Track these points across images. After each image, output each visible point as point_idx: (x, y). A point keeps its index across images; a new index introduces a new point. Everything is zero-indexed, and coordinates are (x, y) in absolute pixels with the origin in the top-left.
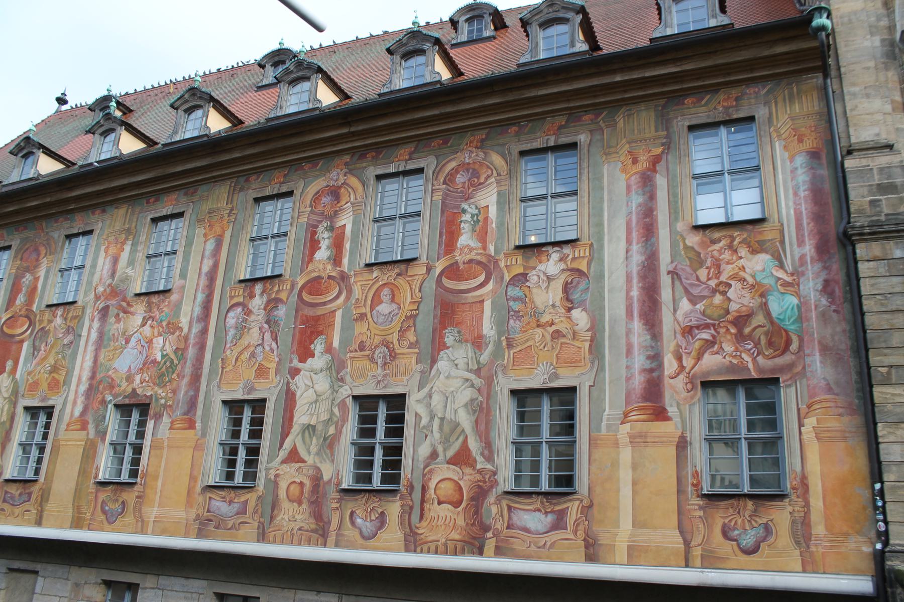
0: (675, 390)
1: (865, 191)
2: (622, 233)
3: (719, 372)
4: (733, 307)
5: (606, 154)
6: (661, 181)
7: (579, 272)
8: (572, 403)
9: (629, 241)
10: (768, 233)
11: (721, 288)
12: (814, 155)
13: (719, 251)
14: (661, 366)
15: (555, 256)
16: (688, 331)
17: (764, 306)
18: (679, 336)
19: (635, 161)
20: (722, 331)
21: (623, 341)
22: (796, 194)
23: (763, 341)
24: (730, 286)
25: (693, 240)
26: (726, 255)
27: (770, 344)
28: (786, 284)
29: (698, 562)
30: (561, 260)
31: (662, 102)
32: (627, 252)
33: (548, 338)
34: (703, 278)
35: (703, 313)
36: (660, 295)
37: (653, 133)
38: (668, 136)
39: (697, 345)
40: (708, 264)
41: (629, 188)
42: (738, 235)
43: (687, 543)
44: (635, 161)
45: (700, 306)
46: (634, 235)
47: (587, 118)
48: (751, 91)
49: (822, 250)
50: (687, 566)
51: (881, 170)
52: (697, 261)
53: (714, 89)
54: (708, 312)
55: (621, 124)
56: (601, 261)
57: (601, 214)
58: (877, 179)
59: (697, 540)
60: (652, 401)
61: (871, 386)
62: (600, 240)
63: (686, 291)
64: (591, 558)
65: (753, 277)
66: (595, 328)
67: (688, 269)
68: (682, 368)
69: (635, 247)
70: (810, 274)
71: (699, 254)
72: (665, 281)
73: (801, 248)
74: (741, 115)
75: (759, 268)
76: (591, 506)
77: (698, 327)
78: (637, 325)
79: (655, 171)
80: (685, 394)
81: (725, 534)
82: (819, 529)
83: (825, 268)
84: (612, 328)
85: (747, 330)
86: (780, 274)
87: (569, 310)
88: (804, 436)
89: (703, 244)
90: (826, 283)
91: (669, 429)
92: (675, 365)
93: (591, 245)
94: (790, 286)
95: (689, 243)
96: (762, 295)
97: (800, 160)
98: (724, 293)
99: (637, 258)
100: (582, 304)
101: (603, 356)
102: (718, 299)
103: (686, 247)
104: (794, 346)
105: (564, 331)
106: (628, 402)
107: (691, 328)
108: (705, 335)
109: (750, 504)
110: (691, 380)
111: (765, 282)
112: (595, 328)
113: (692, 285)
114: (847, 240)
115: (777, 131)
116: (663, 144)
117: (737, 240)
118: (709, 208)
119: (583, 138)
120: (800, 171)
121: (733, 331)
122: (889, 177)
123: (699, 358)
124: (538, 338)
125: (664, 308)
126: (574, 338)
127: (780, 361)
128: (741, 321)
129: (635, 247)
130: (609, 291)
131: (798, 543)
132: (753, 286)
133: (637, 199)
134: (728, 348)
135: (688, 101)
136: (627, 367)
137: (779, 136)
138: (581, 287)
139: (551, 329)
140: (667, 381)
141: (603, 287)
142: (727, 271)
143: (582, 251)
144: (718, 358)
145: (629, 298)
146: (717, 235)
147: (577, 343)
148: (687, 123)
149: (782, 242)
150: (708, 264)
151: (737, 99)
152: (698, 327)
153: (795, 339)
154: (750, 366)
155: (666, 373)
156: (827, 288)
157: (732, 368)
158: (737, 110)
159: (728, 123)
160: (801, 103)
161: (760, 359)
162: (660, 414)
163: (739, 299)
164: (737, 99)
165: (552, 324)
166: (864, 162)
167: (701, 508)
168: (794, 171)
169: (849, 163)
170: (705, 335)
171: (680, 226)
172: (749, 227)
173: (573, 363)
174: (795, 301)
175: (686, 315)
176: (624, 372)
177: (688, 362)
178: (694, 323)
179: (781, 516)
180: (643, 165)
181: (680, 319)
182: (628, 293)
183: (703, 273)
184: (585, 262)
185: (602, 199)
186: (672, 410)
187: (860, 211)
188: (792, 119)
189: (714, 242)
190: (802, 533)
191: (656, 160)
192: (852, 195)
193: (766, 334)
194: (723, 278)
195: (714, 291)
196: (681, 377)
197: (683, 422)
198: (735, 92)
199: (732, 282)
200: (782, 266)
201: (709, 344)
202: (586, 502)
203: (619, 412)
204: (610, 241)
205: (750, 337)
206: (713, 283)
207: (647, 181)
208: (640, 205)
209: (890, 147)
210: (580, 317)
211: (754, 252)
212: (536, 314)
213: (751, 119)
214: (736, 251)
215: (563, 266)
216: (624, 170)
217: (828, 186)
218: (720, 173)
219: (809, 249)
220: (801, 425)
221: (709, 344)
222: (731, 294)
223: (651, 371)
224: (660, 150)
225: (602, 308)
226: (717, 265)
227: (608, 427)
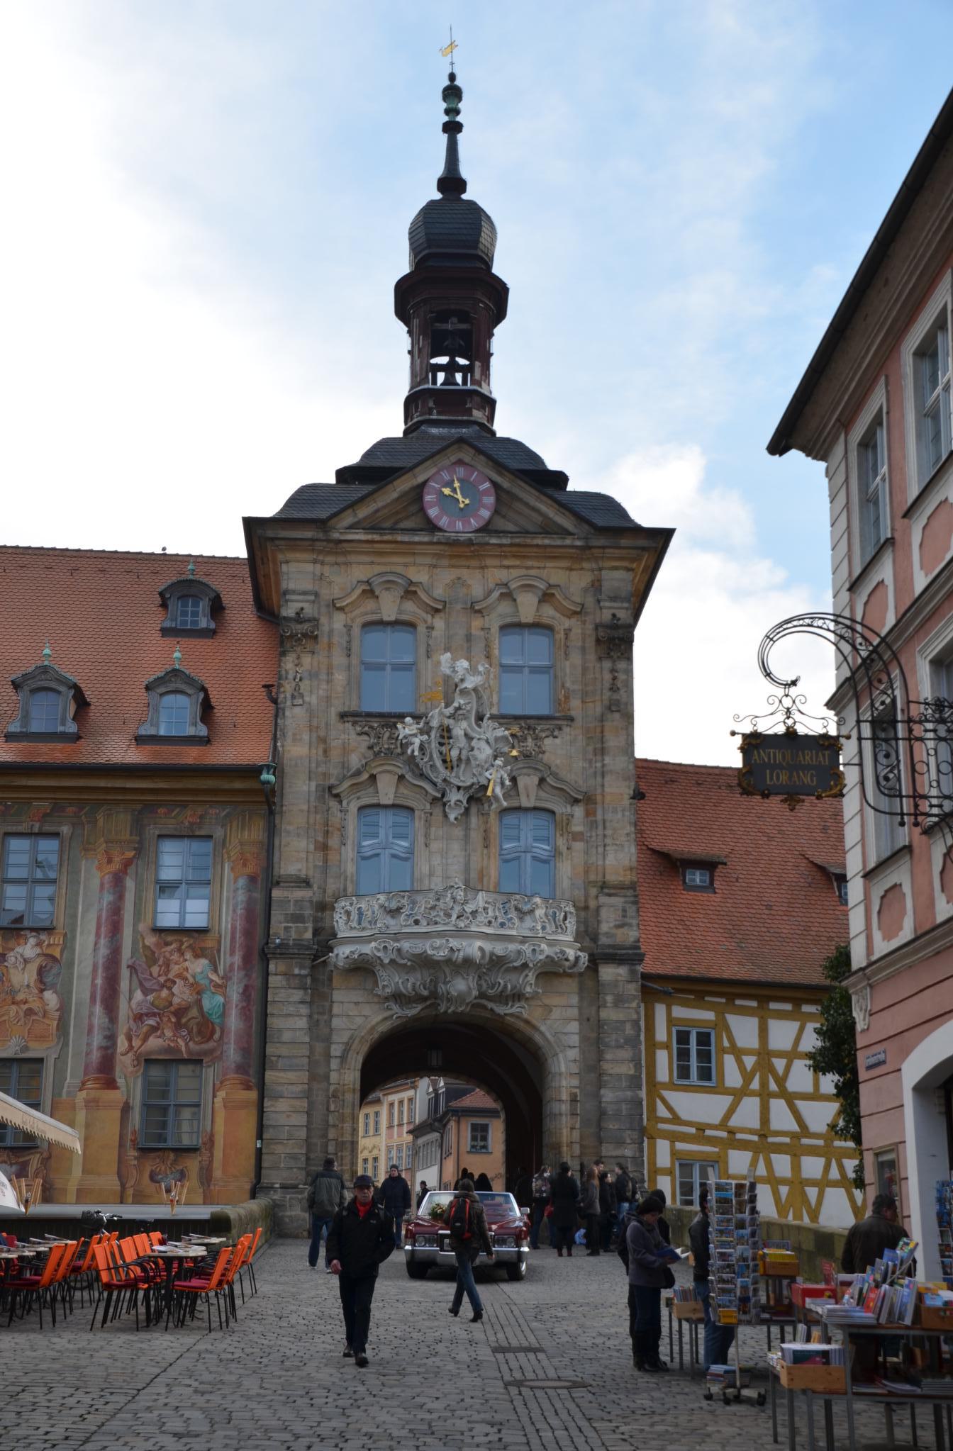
0: (125, 1064)
1: (282, 918)
2: (92, 927)
3: (161, 1051)
4: (176, 1000)
5: (86, 850)
6: (130, 884)
7: (53, 958)
8: (39, 1072)
9: (98, 935)
10: (210, 943)
11: (168, 984)
12: (252, 879)
13: (171, 953)
14: (114, 1045)
15: (32, 941)
16: (139, 1018)
17: (199, 1003)
18: (131, 1021)
19: (110, 861)
20: (165, 1019)
21: (86, 1021)
22: (234, 911)
23: (195, 1030)
24: (175, 983)
25: (151, 940)
26: (175, 957)
27: (200, 1032)
28: (217, 986)
29: (130, 1200)
30: (37, 945)
31: (139, 807)
32: (96, 944)
33: (22, 1014)
34: (155, 975)
35: (152, 1004)
36: (119, 984)
37: (128, 837)
38: (141, 842)
39: (145, 1029)
40: (161, 962)
41: (102, 885)
42: (187, 941)
43: (123, 1186)
44: (110, 861)
45: (150, 998)
46: (103, 929)
47: (71, 810)
48: (212, 811)
49: (247, 959)
50: (121, 1202)
51: (296, 901)
52: (152, 960)
53: (184, 805)
54: (156, 1003)
55: (101, 822)
56: (73, 951)
57: (76, 908)
58: (291, 910)
59: (131, 1182)
60: (105, 1073)
61: (264, 1070)
62: (74, 930)
63: (141, 985)
64: (46, 1199)
65: (194, 977)
66: (64, 1009)
67: (144, 966)
68: (131, 1047)
69: (102, 941)
70: (235, 979)
71: (153, 953)
72: (125, 973)
73: (231, 959)
74: (202, 833)
75: (199, 970)
76: (50, 1157)
77: (147, 1015)
78: (98, 1009)
79: (125, 872)
80: (131, 1069)
81: (152, 1178)
82: (217, 1173)
83: (246, 975)
84: (77, 1011)
85: (184, 1020)
86: (214, 977)
87: (42, 991)
88: (216, 1105)
89: (157, 945)
90: (246, 988)
91: (116, 1096)
92: (126, 1044)
93: (65, 935)
94: (221, 988)
95: (147, 943)
96: (199, 993)
97: (242, 882)
98: (170, 989)
99: (103, 951)
100: (53, 987)
101: (68, 1034)
102: (165, 993)
103: (145, 946)
104: (217, 1036)
105: (36, 1009)
106: (85, 1074)
107: (142, 1015)
108: (152, 1022)
109: (172, 1156)
110: (137, 1058)
111: (202, 982)
112: (64, 1009)
113: (145, 979)
114: (265, 958)
115: (228, 853)
116: (135, 849)
117: (185, 945)
118: (169, 913)
119: (65, 830)
120: (240, 892)
121: (173, 1020)
122: (301, 909)
123: (145, 1040)
124: (12, 1014)
125: (122, 997)
126: (44, 1016)
127: (205, 1046)
128: (180, 1012)
129: (102, 941)
130: (79, 977)
131: (202, 1183)
132: (192, 985)
133: (108, 898)
134: (168, 1033)
135: (161, 811)
136: (88, 1044)
137: (229, 858)
138: (54, 971)
139: (25, 1007)
140: (119, 1058)
141: (72, 974)
142: (175, 969)
143: (57, 939)
144: (160, 1040)
145: (93, 985)
146: (170, 938)
147: (46, 1021)
148: (157, 833)
149: (219, 951)
150: (161, 962)
151: (201, 817)
152: (147, 1015)
153: (218, 1029)
154: (183, 1049)
155: (119, 1050)
156: (246, 992)
157: (168, 1050)
158: (200, 828)
159: (189, 837)
160: (250, 830)
161: (191, 1044)
162: (111, 1084)
163: (181, 994)
164: (201, 817)
165: (25, 1002)
166: (286, 893)
167: (136, 1158)
168: (236, 890)
169: (276, 893)
170: (152, 1022)
171: (141, 927)
172: (196, 935)
173: (41, 1038)
174: (221, 999)
175: (139, 1004)
176: (84, 1048)
177: (136, 1043)
178: (144, 1011)
179: (193, 1165)
180: (116, 866)
181: (134, 1006)
182: (94, 979)
183: (155, 970)
184: (58, 949)
185: (78, 893)
186: (120, 1081)
187: (276, 934)
188: (241, 844)
189: (167, 944)
190: (206, 1176)
191: (127, 864)
192: (273, 919)
193: (198, 1024)
194: (171, 976)
195: (163, 986)
196: (130, 1054)
197: (128, 1091)
198: (200, 810)
199: (177, 980)
200: (216, 970)
201: (154, 1029)
202: (45, 1155)
203: (77, 1082)
204: (82, 933)
205: (185, 1026)
206: (162, 979)
207: (118, 881)
208: (110, 903)
209: (306, 883)
210: (51, 998)
211: (197, 956)
212: (12, 992)
213: (211, 837)
214: (182, 954)
215: (38, 951)
216: (99, 868)
217: (259, 908)
218: (179, 882)
219: (237, 959)
220: (214, 1096)
221: (154, 1029)
222: (175, 990)
223: (106, 1048)
224: (133, 853)
225: (70, 992)
226: (167, 964)
227: (69, 1093)
